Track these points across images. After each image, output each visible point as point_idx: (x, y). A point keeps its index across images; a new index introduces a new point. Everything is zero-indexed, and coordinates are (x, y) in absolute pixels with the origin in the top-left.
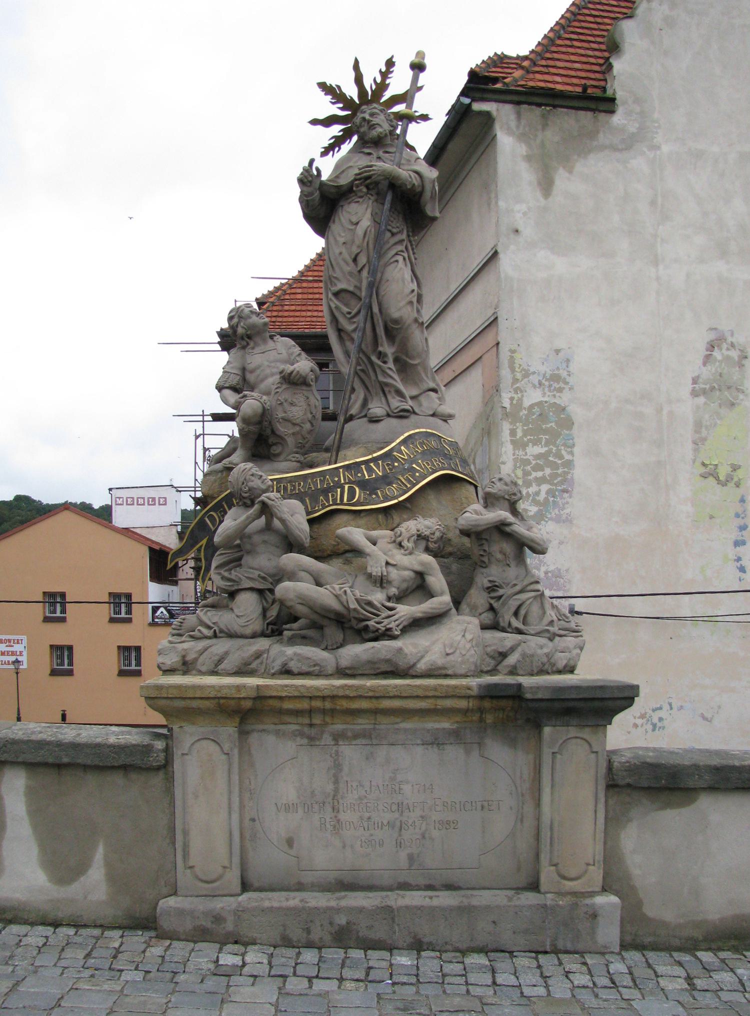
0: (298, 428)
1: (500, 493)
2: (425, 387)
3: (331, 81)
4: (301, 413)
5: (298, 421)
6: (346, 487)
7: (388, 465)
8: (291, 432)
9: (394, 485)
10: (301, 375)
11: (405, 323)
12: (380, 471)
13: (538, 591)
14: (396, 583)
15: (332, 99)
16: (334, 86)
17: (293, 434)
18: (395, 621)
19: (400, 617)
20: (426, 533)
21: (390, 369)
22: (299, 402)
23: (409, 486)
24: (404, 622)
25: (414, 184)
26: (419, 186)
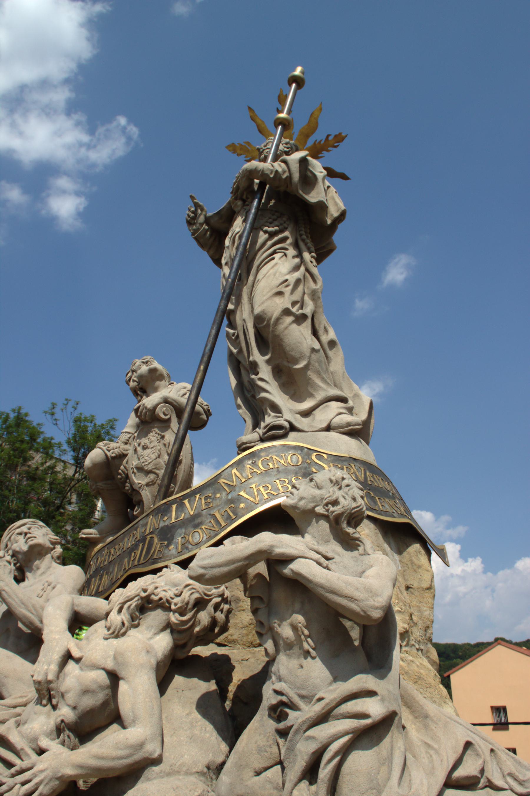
0: (152, 476)
1: (302, 503)
2: (320, 396)
3: (238, 140)
4: (153, 457)
5: (150, 467)
6: (148, 537)
7: (206, 498)
8: (143, 483)
9: (203, 527)
10: (146, 408)
11: (270, 319)
12: (192, 509)
13: (364, 716)
14: (71, 698)
15: (246, 157)
16: (243, 144)
17: (148, 485)
18: (23, 784)
19: (35, 775)
20: (162, 594)
21: (261, 379)
22: (151, 442)
23: (223, 524)
24: (41, 788)
25: (277, 171)
26: (284, 172)
